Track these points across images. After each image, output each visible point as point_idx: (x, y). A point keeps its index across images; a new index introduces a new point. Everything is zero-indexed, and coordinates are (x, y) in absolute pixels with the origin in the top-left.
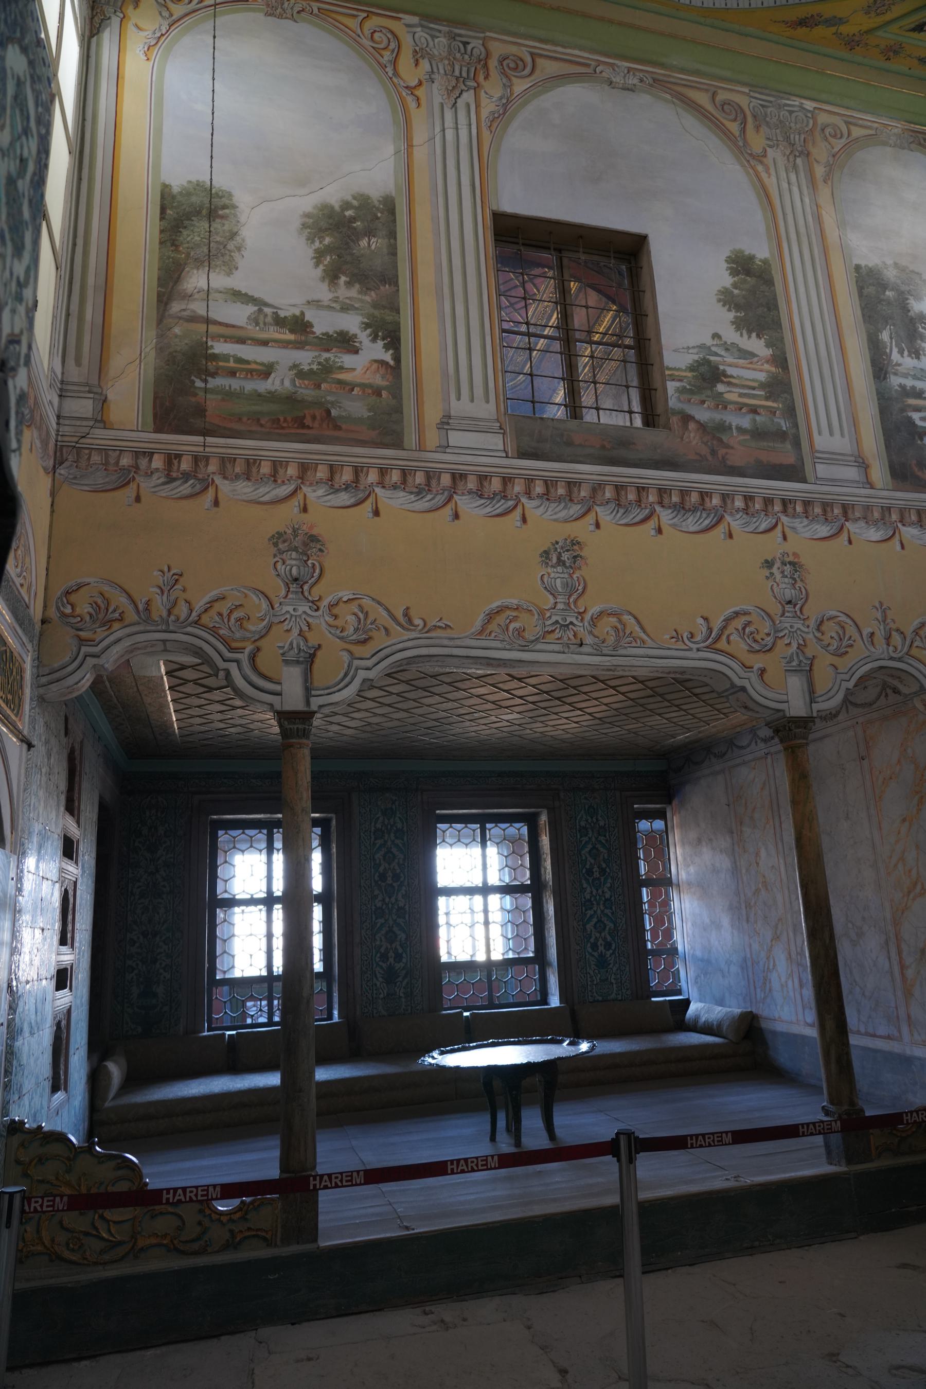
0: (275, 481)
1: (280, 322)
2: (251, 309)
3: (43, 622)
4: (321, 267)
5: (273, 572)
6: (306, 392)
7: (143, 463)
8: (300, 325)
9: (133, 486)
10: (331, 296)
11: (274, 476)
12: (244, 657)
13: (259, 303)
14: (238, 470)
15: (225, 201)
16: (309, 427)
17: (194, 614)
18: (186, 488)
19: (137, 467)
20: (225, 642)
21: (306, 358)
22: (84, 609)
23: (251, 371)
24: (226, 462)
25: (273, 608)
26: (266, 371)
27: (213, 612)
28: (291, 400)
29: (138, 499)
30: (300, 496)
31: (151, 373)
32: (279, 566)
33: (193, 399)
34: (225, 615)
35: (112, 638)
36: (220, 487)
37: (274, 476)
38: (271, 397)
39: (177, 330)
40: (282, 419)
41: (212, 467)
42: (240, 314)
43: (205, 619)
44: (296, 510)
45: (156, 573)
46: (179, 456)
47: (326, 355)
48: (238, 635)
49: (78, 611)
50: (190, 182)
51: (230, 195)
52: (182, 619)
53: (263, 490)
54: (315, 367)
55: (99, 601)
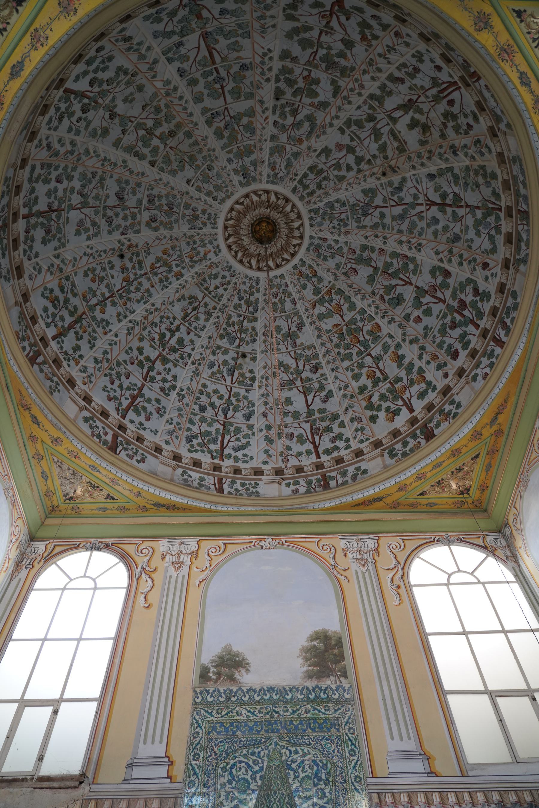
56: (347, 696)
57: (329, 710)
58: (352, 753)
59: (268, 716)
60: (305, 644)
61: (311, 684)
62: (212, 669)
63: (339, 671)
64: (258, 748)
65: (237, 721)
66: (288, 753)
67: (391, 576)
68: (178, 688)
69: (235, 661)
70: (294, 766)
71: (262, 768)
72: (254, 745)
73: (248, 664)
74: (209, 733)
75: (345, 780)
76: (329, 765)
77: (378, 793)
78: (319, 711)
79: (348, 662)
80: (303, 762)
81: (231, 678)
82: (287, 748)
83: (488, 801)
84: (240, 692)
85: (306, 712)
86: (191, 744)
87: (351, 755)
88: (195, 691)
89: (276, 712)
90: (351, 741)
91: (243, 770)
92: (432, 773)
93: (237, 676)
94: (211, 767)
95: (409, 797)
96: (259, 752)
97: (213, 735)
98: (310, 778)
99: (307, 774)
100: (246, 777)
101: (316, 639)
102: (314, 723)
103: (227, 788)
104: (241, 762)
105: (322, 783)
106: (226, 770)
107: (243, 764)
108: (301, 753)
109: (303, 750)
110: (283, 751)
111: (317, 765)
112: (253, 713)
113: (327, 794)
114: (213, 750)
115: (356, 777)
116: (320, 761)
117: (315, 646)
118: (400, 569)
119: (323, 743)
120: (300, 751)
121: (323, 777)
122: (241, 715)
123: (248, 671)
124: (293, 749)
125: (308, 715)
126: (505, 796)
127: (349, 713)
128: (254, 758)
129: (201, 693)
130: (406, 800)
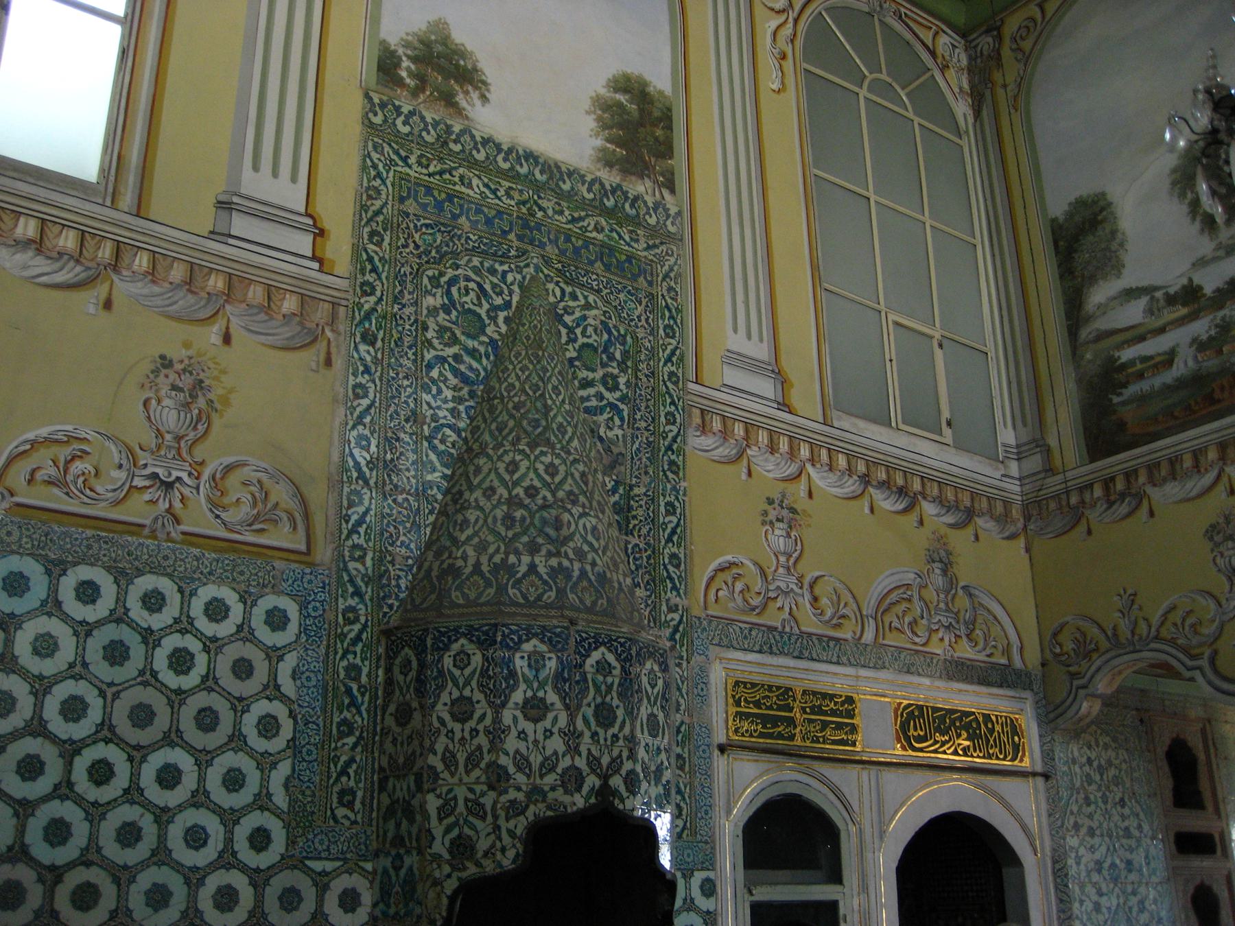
0: (1199, 471)
1: (1171, 300)
2: (1144, 301)
3: (1043, 665)
4: (1199, 218)
5: (1215, 569)
6: (1211, 363)
7: (1087, 496)
8: (1190, 294)
9: (1084, 521)
10: (1213, 245)
11: (1197, 465)
12: (1204, 663)
13: (1148, 290)
14: (1163, 473)
15: (1102, 203)
16: (1219, 401)
17: (1153, 629)
18: (1123, 509)
19: (1083, 502)
20: (1185, 650)
21: (1202, 327)
22: (1069, 646)
23: (1156, 366)
24: (1153, 468)
25: (1220, 606)
26: (1169, 359)
27: (1168, 624)
28: (1197, 380)
29: (1089, 532)
30: (1225, 479)
31: (1077, 406)
32: (1218, 560)
33: (1114, 418)
34: (1179, 623)
35: (1093, 668)
36: (1152, 496)
37: (1197, 465)
38: (1181, 384)
39: (1088, 356)
40: (1193, 403)
41: (1142, 479)
42: (1134, 313)
43: (1164, 633)
44: (1224, 495)
45: (1116, 598)
46: (1113, 479)
47: (1221, 314)
48: (1194, 641)
49: (1065, 649)
50: (1070, 204)
51: (1103, 194)
52: (1145, 634)
53: (1189, 485)
54: (1213, 332)
55: (1078, 635)
56: (672, 229)
57: (637, 241)
58: (670, 332)
59: (524, 210)
60: (603, 91)
61: (610, 178)
62: (406, 63)
63: (662, 175)
64: (502, 263)
65: (460, 196)
66: (558, 293)
67: (773, 24)
68: (329, 76)
69: (457, 66)
70: (567, 319)
71: (508, 305)
72: (495, 254)
73: (484, 83)
74: (402, 200)
75: (653, 373)
76: (629, 339)
77: (702, 411)
78: (621, 237)
79: (678, 162)
80: (584, 318)
81: (448, 100)
82: (557, 283)
83: (850, 470)
84: (467, 138)
85: (596, 228)
86: (365, 208)
87: (667, 335)
88: (367, 96)
89: (541, 209)
90: (670, 311)
91: (472, 294)
92: (784, 406)
93: (460, 99)
94: (407, 269)
95: (747, 431)
96: (505, 273)
97: (411, 206)
98: (595, 350)
99: (590, 341)
100: (477, 309)
101: (625, 91)
102: (610, 256)
103: (440, 319)
104: (468, 279)
105: (615, 364)
106: (438, 286)
107: (472, 285)
108: (583, 302)
109: (586, 297)
110: (550, 286)
111: (610, 333)
112: (494, 192)
113: (622, 387)
114: (410, 236)
115: (671, 374)
116: (615, 327)
117: (620, 105)
118: (791, 20)
119: (622, 296)
120: (581, 297)
121: (618, 356)
122: (470, 186)
123: (484, 99)
124: (569, 289)
125: (600, 237)
126: (873, 469)
127: (672, 260)
128: (495, 280)
129: (383, 105)
130: (742, 433)
